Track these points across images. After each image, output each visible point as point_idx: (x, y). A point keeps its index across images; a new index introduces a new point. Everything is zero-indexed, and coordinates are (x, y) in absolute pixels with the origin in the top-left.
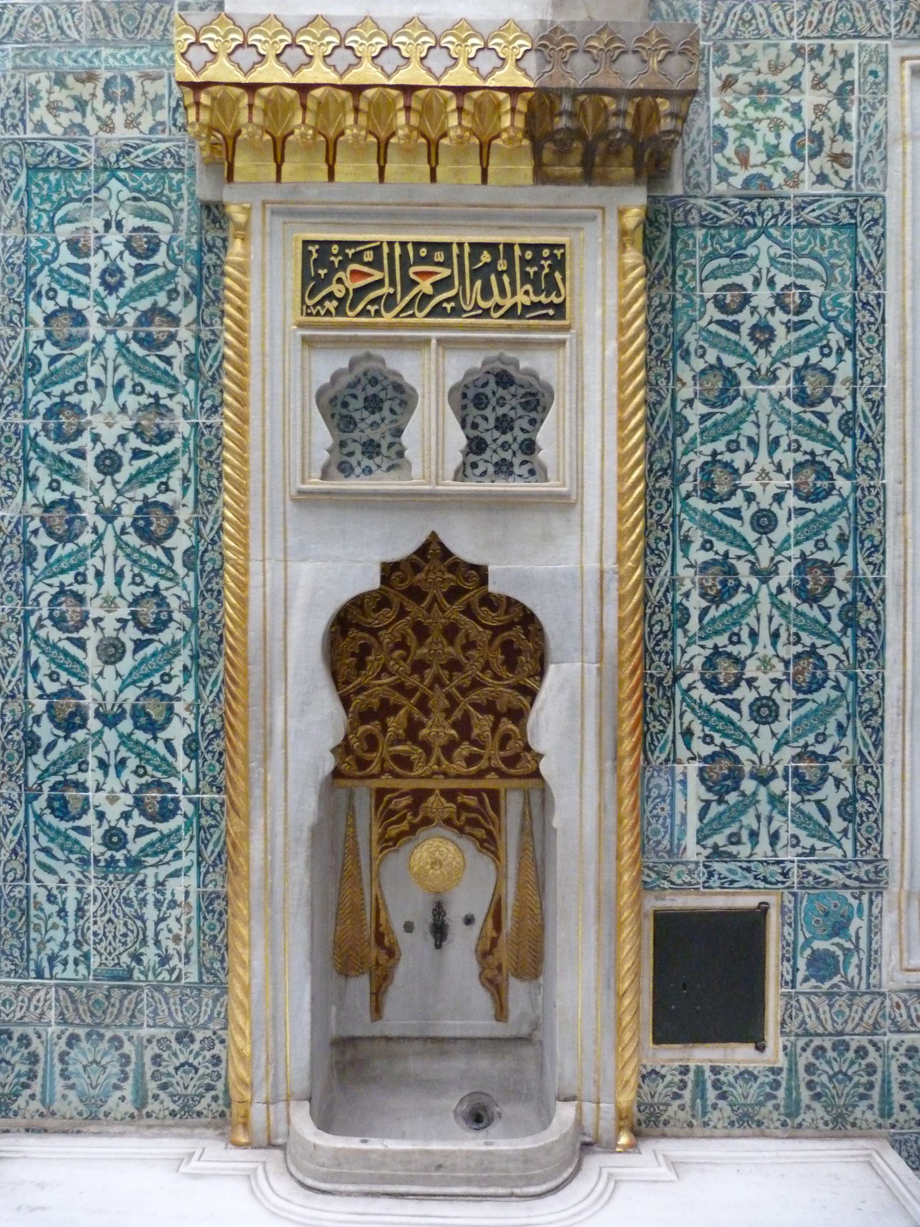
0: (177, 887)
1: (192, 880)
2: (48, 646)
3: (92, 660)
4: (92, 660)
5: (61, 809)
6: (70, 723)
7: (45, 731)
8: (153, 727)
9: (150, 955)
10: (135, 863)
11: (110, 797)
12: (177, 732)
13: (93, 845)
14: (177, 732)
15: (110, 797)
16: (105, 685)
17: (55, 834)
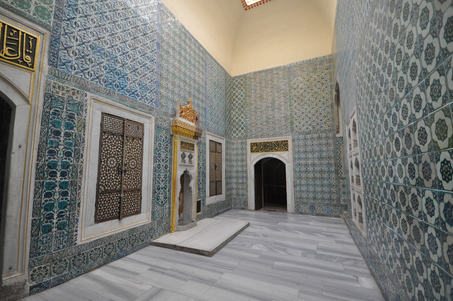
0: (167, 206)
1: (168, 205)
2: (157, 181)
3: (161, 182)
4: (161, 182)
5: (158, 200)
6: (159, 189)
7: (157, 191)
8: (165, 189)
9: (165, 215)
10: (164, 204)
11: (162, 197)
12: (167, 189)
13: (160, 203)
14: (167, 189)
15: (162, 197)
16: (162, 185)
17: (157, 203)
